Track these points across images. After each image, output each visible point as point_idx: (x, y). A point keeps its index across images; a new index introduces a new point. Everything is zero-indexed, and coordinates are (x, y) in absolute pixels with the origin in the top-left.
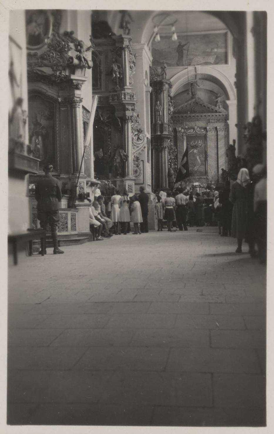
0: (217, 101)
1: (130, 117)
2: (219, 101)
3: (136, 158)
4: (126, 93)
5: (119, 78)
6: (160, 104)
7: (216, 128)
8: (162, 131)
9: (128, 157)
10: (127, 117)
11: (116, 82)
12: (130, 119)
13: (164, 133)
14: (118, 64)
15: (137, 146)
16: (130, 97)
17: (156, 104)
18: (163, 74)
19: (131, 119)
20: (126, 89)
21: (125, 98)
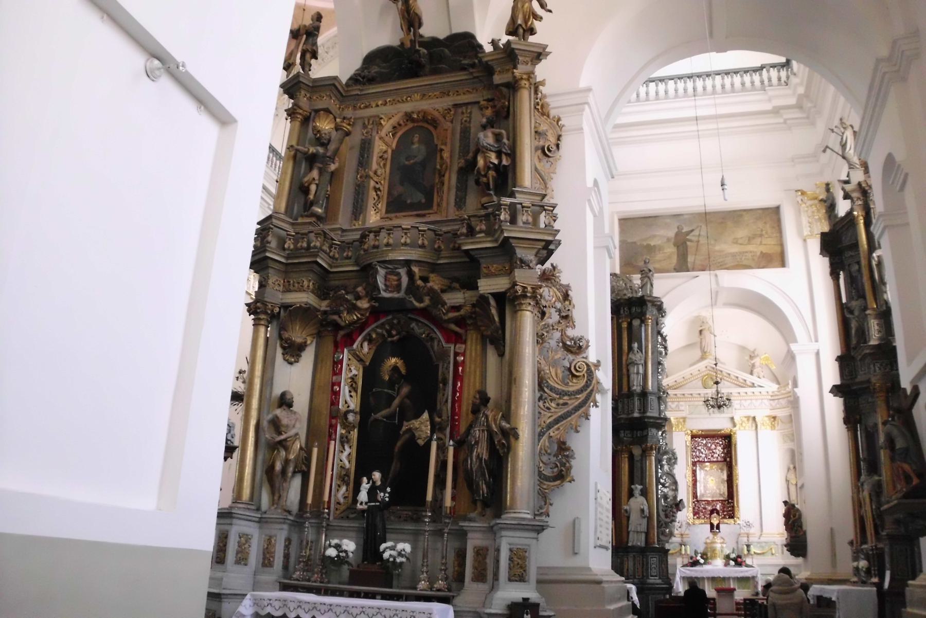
0: (753, 366)
1: (529, 289)
2: (757, 364)
3: (556, 447)
4: (519, 206)
5: (497, 168)
6: (640, 348)
7: (754, 418)
8: (644, 408)
9: (517, 437)
10: (518, 288)
11: (488, 184)
12: (529, 295)
13: (649, 414)
14: (497, 131)
15: (561, 401)
16: (530, 219)
17: (630, 349)
18: (647, 283)
19: (534, 297)
20: (517, 195)
21: (513, 221)
